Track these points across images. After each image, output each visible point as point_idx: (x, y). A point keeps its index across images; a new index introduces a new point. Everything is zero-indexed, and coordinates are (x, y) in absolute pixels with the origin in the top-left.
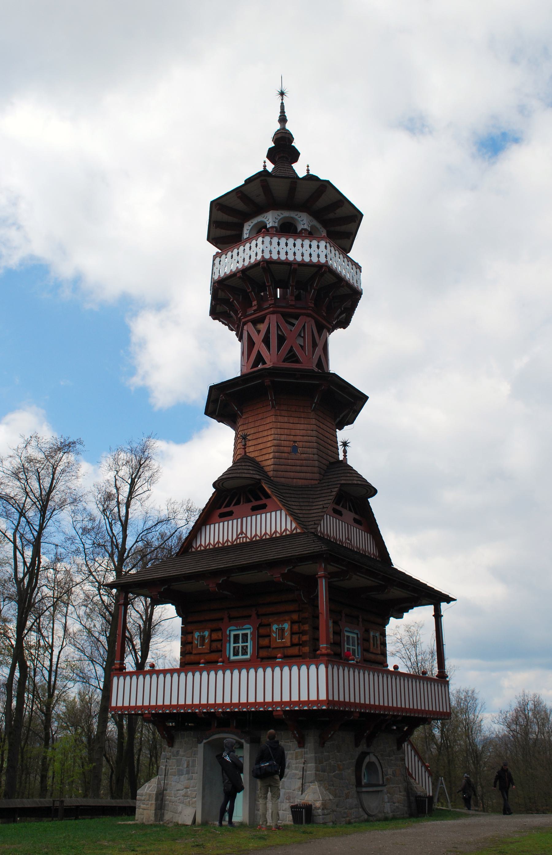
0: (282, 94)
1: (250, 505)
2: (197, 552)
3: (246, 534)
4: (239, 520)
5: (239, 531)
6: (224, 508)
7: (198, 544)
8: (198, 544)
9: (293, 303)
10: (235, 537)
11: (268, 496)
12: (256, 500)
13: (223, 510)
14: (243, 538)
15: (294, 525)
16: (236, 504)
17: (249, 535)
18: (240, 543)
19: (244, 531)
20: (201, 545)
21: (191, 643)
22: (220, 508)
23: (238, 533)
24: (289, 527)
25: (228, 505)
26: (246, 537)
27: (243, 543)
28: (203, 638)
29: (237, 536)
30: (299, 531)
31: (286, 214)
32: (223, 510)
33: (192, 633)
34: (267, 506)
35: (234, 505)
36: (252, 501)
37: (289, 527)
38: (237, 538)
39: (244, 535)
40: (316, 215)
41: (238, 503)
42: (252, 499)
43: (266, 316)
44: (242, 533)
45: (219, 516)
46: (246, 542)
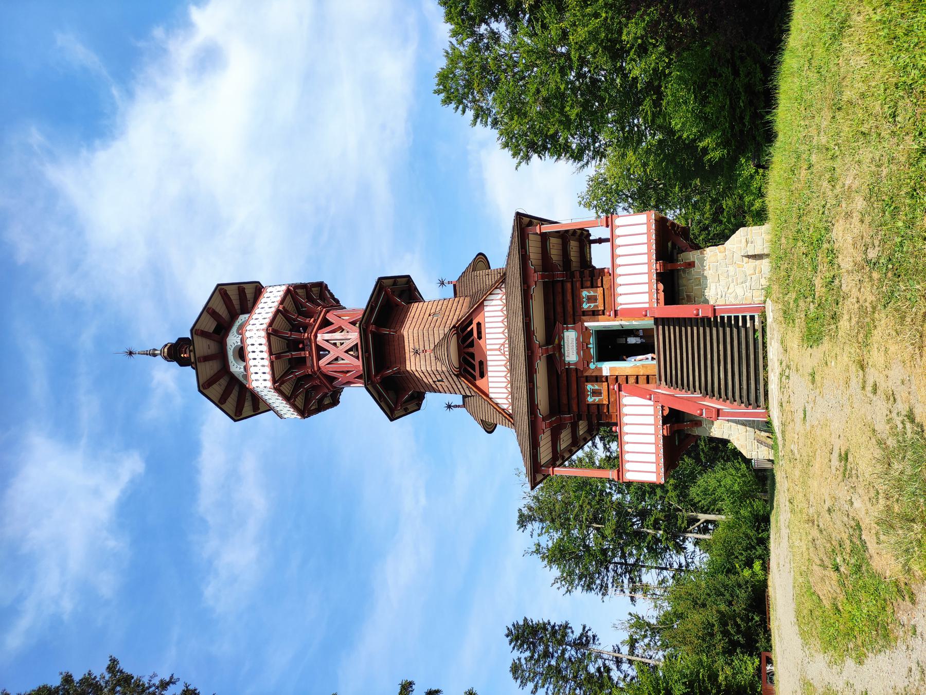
0: (131, 353)
2: (512, 404)
5: (498, 353)
6: (474, 370)
7: (505, 401)
9: (312, 319)
10: (503, 358)
12: (472, 335)
13: (477, 374)
14: (504, 347)
15: (498, 291)
17: (502, 341)
19: (497, 347)
23: (500, 353)
25: (474, 368)
26: (503, 344)
28: (596, 393)
31: (234, 329)
32: (477, 374)
34: (479, 322)
35: (474, 360)
38: (504, 355)
39: (502, 348)
40: (243, 313)
41: (472, 356)
42: (472, 338)
43: (317, 345)
44: (499, 350)
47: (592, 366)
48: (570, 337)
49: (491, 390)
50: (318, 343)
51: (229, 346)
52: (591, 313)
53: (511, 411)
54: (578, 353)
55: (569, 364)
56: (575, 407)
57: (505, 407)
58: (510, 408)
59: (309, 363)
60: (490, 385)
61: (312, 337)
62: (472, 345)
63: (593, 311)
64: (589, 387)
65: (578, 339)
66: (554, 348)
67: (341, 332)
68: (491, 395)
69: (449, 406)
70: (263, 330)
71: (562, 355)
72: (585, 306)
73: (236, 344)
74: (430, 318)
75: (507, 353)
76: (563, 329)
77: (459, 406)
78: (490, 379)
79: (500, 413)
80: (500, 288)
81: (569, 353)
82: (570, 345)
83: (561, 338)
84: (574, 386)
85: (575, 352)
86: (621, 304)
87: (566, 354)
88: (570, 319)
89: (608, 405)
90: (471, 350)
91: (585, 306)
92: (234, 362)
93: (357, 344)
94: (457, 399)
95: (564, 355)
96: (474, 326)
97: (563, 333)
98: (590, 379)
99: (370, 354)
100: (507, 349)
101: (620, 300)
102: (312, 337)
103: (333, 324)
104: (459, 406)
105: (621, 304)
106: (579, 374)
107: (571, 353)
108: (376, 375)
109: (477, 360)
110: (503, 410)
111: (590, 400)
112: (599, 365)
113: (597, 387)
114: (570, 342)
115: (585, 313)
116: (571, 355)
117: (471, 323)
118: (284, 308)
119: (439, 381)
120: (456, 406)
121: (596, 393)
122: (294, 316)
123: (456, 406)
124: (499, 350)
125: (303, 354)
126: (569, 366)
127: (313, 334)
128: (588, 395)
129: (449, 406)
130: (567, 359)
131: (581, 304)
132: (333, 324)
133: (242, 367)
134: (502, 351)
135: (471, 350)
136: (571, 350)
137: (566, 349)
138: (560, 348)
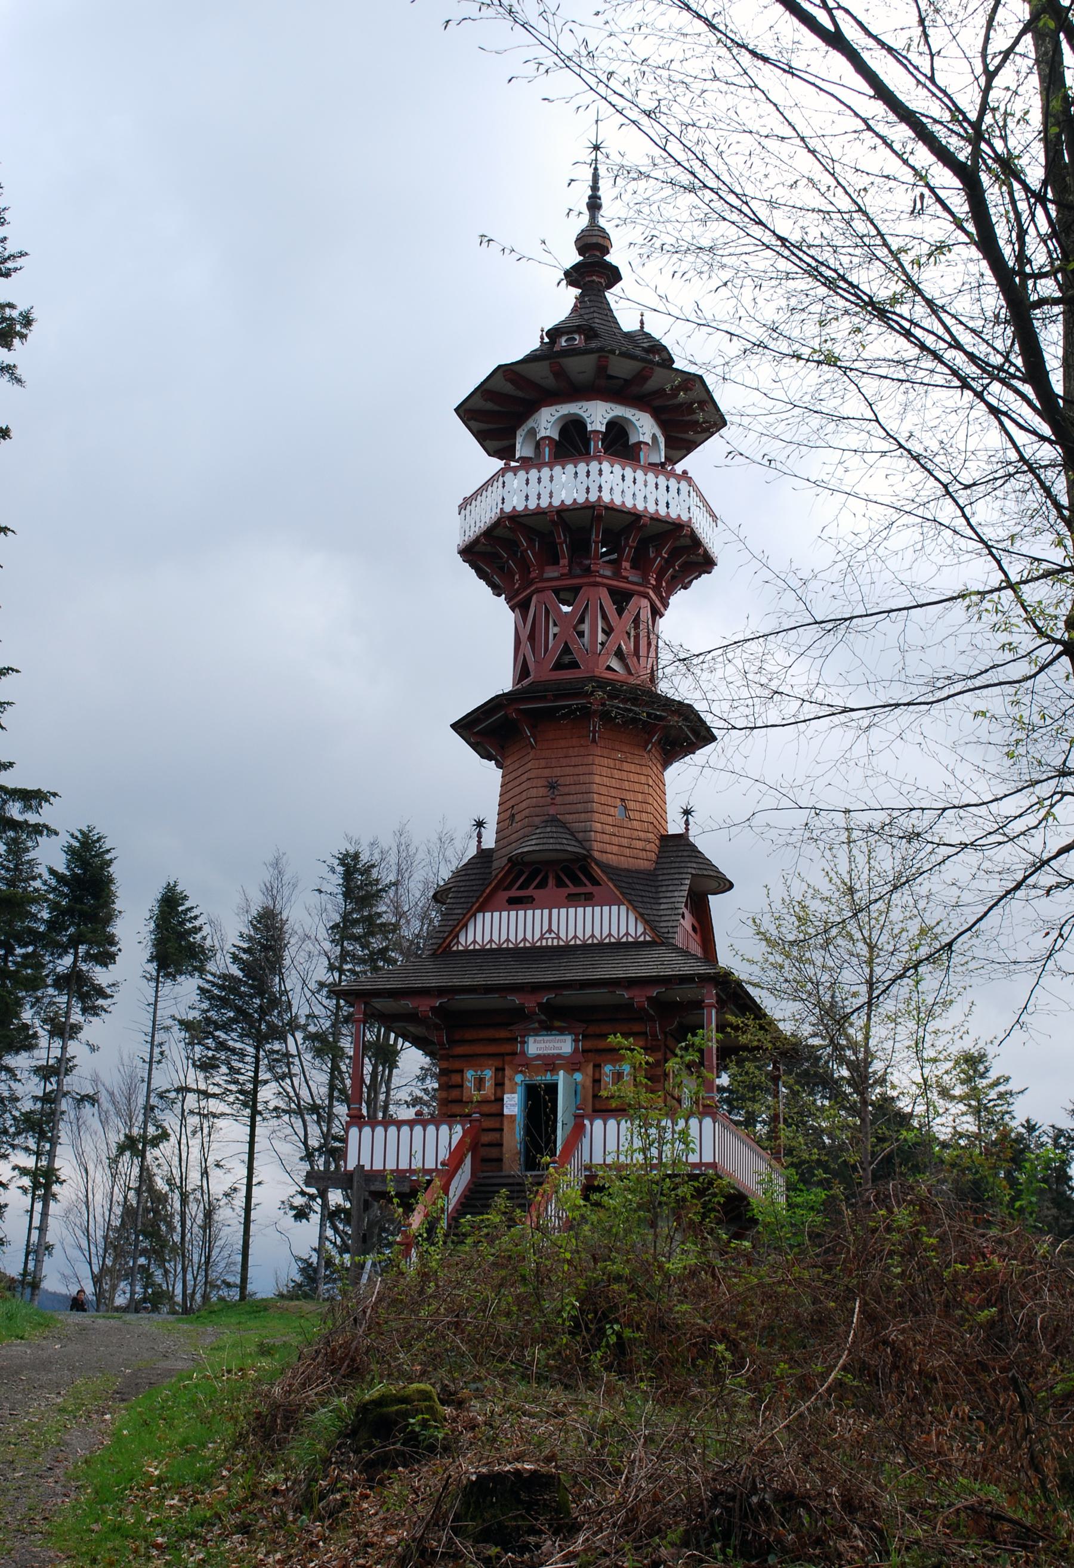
1: (565, 891)
2: (466, 952)
3: (558, 935)
4: (546, 912)
5: (546, 928)
6: (518, 889)
7: (470, 939)
8: (470, 939)
10: (537, 936)
11: (595, 882)
14: (553, 939)
15: (640, 930)
16: (539, 887)
17: (563, 935)
18: (547, 947)
19: (554, 928)
20: (474, 942)
21: (461, 1086)
22: (508, 888)
24: (632, 931)
26: (559, 938)
27: (553, 947)
28: (480, 1082)
29: (542, 935)
30: (648, 938)
32: (514, 893)
33: (462, 1071)
35: (536, 888)
36: (567, 886)
37: (632, 931)
38: (542, 938)
39: (553, 935)
41: (542, 885)
42: (570, 884)
43: (581, 588)
44: (550, 931)
45: (507, 901)
46: (559, 946)
47: (519, 1078)
48: (564, 1045)
49: (488, 915)
50: (584, 589)
51: (586, 405)
52: (597, 1077)
53: (455, 948)
54: (538, 1057)
55: (524, 1043)
56: (460, 1050)
57: (462, 940)
58: (461, 948)
59: (551, 572)
60: (496, 914)
61: (592, 580)
62: (560, 884)
63: (599, 1081)
64: (488, 1074)
65: (559, 1056)
66: (545, 1021)
67: (603, 631)
68: (480, 916)
69: (480, 824)
70: (600, 498)
71: (536, 1033)
72: (608, 1069)
73: (588, 421)
74: (618, 803)
75: (544, 943)
76: (577, 1035)
77: (479, 842)
78: (505, 914)
79: (451, 932)
80: (644, 933)
81: (540, 1042)
82: (551, 1045)
83: (562, 1031)
84: (492, 1049)
85: (539, 1052)
86: (592, 1125)
87: (538, 1038)
88: (590, 1044)
89: (461, 1101)
90: (551, 882)
91: (608, 1069)
92: (558, 415)
93: (574, 665)
94: (489, 841)
95: (537, 1035)
96: (590, 888)
97: (570, 1034)
98: (500, 1070)
99: (553, 701)
100: (550, 944)
101: (598, 1123)
102: (592, 580)
103: (620, 612)
104: (479, 842)
105: (592, 1125)
106: (507, 1058)
107: (539, 1045)
108: (519, 711)
109: (537, 894)
110: (457, 936)
111: (469, 1074)
112: (520, 1090)
113: (487, 1084)
114: (556, 1045)
115: (597, 1067)
116: (536, 1046)
117: (595, 882)
118: (645, 525)
119: (513, 815)
120: (479, 836)
121: (480, 1082)
122: (633, 542)
123: (479, 836)
124: (550, 931)
125: (564, 562)
126: (521, 1042)
127: (599, 579)
128: (476, 1072)
129: (480, 824)
130: (531, 1040)
131: (613, 1062)
132: (620, 612)
133: (548, 434)
134: (547, 935)
135: (551, 882)
136: (543, 1045)
137: (546, 1038)
138: (547, 1028)
